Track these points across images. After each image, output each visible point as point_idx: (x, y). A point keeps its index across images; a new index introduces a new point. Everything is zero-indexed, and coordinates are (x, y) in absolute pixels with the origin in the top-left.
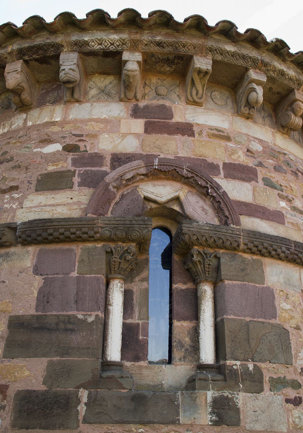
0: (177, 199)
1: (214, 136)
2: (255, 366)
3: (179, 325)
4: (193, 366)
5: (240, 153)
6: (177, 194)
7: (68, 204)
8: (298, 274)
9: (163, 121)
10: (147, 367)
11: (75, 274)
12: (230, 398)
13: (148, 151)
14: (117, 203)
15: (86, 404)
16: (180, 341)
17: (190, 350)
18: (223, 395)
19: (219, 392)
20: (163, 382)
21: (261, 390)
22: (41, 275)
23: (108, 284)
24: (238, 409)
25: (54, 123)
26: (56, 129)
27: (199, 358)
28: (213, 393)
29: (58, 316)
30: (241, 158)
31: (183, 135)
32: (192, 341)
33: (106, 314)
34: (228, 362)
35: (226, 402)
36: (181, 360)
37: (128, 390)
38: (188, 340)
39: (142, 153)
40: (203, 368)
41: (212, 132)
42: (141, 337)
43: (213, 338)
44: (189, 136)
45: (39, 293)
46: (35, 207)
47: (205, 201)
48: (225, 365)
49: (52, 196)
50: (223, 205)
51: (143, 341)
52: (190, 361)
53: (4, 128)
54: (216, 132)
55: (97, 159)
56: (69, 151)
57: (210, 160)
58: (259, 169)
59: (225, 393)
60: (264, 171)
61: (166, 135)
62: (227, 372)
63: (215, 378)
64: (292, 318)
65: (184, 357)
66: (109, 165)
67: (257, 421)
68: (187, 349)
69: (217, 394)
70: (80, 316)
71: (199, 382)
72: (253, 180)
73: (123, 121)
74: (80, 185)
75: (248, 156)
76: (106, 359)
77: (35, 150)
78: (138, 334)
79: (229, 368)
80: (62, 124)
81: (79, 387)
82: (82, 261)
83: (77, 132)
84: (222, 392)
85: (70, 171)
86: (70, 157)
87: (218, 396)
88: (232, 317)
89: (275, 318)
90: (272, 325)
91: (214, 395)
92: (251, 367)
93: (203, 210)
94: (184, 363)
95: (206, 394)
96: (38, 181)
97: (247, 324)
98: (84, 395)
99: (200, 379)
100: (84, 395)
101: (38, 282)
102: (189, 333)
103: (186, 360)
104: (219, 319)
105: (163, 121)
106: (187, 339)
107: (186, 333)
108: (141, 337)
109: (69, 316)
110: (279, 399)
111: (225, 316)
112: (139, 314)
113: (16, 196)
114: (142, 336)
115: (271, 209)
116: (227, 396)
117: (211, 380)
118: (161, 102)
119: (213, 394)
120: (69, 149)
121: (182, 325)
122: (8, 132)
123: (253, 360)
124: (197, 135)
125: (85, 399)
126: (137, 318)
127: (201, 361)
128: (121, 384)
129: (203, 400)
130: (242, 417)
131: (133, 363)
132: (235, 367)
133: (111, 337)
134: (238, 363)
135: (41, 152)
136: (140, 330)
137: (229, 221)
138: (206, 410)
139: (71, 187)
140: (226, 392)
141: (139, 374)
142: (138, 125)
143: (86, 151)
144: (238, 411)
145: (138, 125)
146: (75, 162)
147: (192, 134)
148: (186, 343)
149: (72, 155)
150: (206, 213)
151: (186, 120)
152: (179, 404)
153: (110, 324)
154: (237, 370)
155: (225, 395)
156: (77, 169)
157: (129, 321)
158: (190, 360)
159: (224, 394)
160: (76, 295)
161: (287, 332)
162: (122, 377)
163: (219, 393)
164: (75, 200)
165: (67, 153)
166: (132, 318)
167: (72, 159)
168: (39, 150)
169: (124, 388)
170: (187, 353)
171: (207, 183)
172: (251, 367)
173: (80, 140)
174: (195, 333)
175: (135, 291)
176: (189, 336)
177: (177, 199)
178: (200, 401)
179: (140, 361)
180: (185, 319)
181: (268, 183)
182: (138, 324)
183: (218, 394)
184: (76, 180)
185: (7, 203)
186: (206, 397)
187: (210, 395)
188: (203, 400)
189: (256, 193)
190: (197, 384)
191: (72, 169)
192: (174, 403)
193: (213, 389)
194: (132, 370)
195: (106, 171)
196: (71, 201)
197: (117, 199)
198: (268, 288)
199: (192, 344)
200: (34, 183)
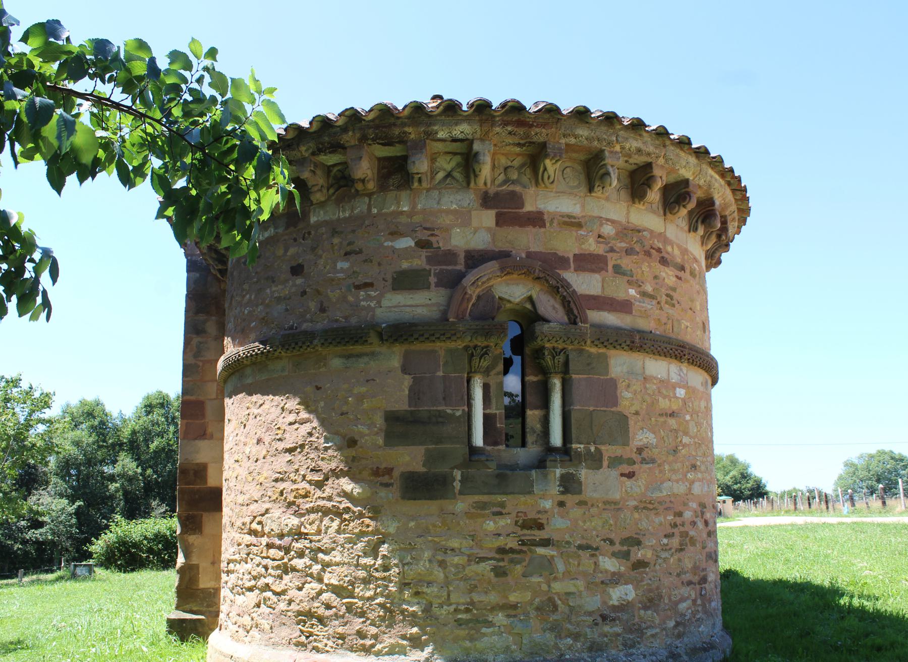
0: (530, 299)
1: (565, 223)
2: (596, 448)
5: (591, 241)
6: (529, 294)
7: (427, 305)
8: (642, 362)
9: (514, 211)
11: (440, 374)
13: (501, 246)
14: (473, 305)
15: (460, 481)
16: (532, 428)
21: (601, 467)
22: (409, 374)
23: (469, 381)
24: (581, 482)
25: (402, 213)
26: (403, 219)
29: (429, 411)
30: (592, 246)
31: (534, 226)
34: (574, 446)
39: (495, 249)
41: (564, 219)
44: (540, 227)
45: (409, 391)
46: (395, 307)
47: (555, 299)
48: (571, 447)
49: (411, 296)
50: (572, 305)
53: (344, 211)
54: (567, 220)
55: (450, 256)
56: (422, 247)
57: (560, 254)
58: (609, 255)
60: (614, 255)
61: (517, 228)
62: (573, 453)
63: (563, 459)
64: (632, 405)
65: (536, 441)
66: (463, 263)
67: (595, 491)
69: (564, 471)
70: (449, 411)
72: (602, 269)
73: (473, 213)
74: (437, 285)
75: (599, 243)
76: (472, 446)
77: (386, 244)
78: (495, 422)
80: (410, 214)
81: (453, 468)
82: (446, 364)
83: (428, 225)
85: (425, 270)
86: (424, 253)
88: (578, 407)
89: (617, 406)
90: (613, 412)
92: (593, 449)
93: (554, 308)
95: (555, 472)
96: (394, 279)
97: (591, 412)
98: (458, 474)
99: (550, 461)
100: (458, 474)
101: (407, 381)
104: (567, 409)
105: (514, 211)
106: (538, 426)
109: (439, 411)
110: (614, 473)
111: (572, 407)
113: (373, 293)
115: (619, 299)
118: (511, 188)
120: (422, 244)
122: (350, 217)
123: (594, 444)
124: (548, 225)
125: (459, 477)
130: (583, 487)
132: (579, 450)
134: (582, 446)
135: (392, 246)
137: (578, 320)
138: (555, 483)
139: (428, 288)
142: (488, 217)
143: (439, 248)
144: (580, 483)
145: (488, 217)
146: (429, 260)
147: (543, 225)
149: (427, 252)
150: (557, 312)
151: (537, 208)
154: (581, 452)
156: (433, 268)
157: (488, 411)
160: (444, 391)
161: (627, 418)
162: (487, 460)
164: (433, 301)
165: (420, 249)
166: (490, 409)
167: (426, 257)
168: (390, 244)
169: (490, 469)
171: (558, 283)
172: (593, 449)
173: (432, 235)
174: (546, 421)
175: (491, 384)
177: (530, 299)
178: (551, 477)
180: (536, 408)
181: (618, 270)
182: (496, 414)
184: (433, 280)
185: (363, 300)
187: (558, 472)
189: (605, 285)
190: (548, 464)
191: (428, 267)
195: (460, 270)
196: (429, 302)
197: (473, 300)
198: (612, 379)
200: (390, 281)
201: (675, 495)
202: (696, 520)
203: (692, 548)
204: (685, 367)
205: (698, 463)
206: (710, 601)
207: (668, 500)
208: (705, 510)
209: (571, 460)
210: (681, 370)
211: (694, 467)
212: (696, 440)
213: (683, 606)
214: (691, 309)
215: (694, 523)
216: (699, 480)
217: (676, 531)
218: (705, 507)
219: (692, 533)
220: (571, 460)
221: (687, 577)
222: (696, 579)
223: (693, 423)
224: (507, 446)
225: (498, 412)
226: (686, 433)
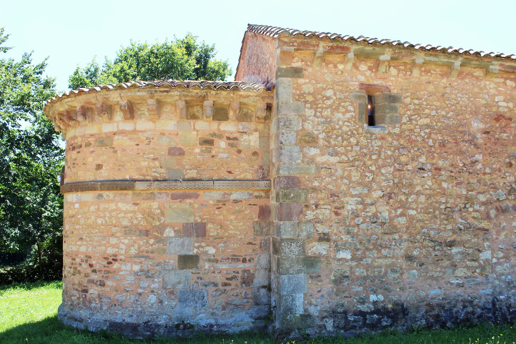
201: (73, 251)
202: (81, 263)
203: (78, 275)
204: (79, 194)
205: (84, 237)
206: (90, 302)
207: (71, 253)
208: (89, 259)
210: (78, 195)
211: (82, 239)
212: (84, 226)
213: (73, 298)
214: (84, 164)
215: (80, 264)
216: (85, 245)
217: (72, 266)
218: (91, 258)
219: (79, 269)
221: (76, 287)
222: (80, 289)
223: (83, 218)
226: (78, 224)
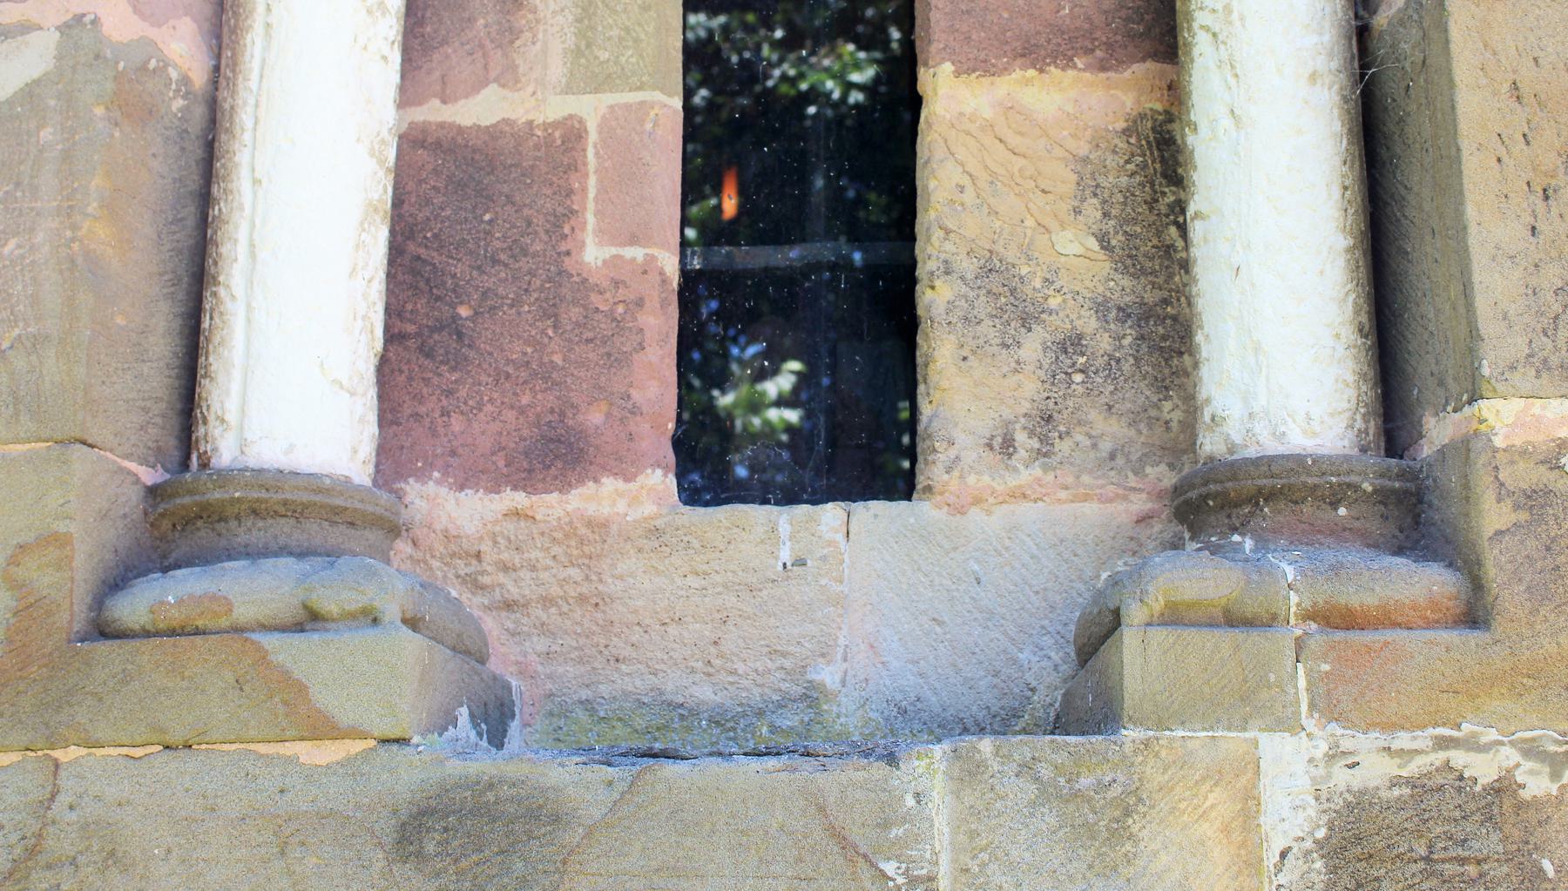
3: (987, 113)
4: (1140, 504)
10: (656, 532)
12: (1536, 803)
17: (1105, 343)
18: (1447, 766)
19: (1403, 740)
20: (828, 676)
27: (1191, 405)
28: (1324, 747)
32: (1129, 263)
33: (226, 40)
35: (1489, 843)
36: (1008, 446)
37: (358, 746)
38: (1079, 250)
40: (1228, 504)
42: (600, 244)
43: (1336, 192)
51: (617, 283)
52: (1112, 457)
59: (1472, 744)
63: (1354, 596)
68: (1071, 344)
71: (1159, 635)
76: (204, 465)
78: (562, 221)
79: (1525, 475)
84: (1443, 743)
87: (1395, 782)
91: (1342, 778)
94: (1038, 480)
99: (1175, 617)
102: (1089, 187)
103: (1063, 447)
107: (1064, 179)
108: (593, 253)
112: (580, 34)
114: (608, 235)
116: (1503, 788)
117: (1309, 616)
119: (1331, 758)
121: (1009, 109)
126: (557, 70)
127: (1210, 445)
128: (292, 691)
129: (1207, 829)
131: (519, 499)
133: (252, 246)
136: (592, 181)
140: (1492, 735)
141: (582, 599)
148: (1063, 281)
152: (931, 879)
153: (245, 118)
155: (1483, 769)
158: (1106, 446)
159: (1458, 758)
162: (310, 620)
163: (1407, 754)
166: (509, 78)
169: (322, 729)
170: (1078, 378)
176: (1092, 210)
179: (581, 481)
182: (572, 133)
183: (1391, 767)
186: (1249, 806)
188: (1207, 829)
192: (873, 865)
193: (1328, 707)
194: (505, 568)
199: (1123, 288)
209: (1473, 616)
220: (1473, 616)
224: (691, 496)
225: (590, 109)
